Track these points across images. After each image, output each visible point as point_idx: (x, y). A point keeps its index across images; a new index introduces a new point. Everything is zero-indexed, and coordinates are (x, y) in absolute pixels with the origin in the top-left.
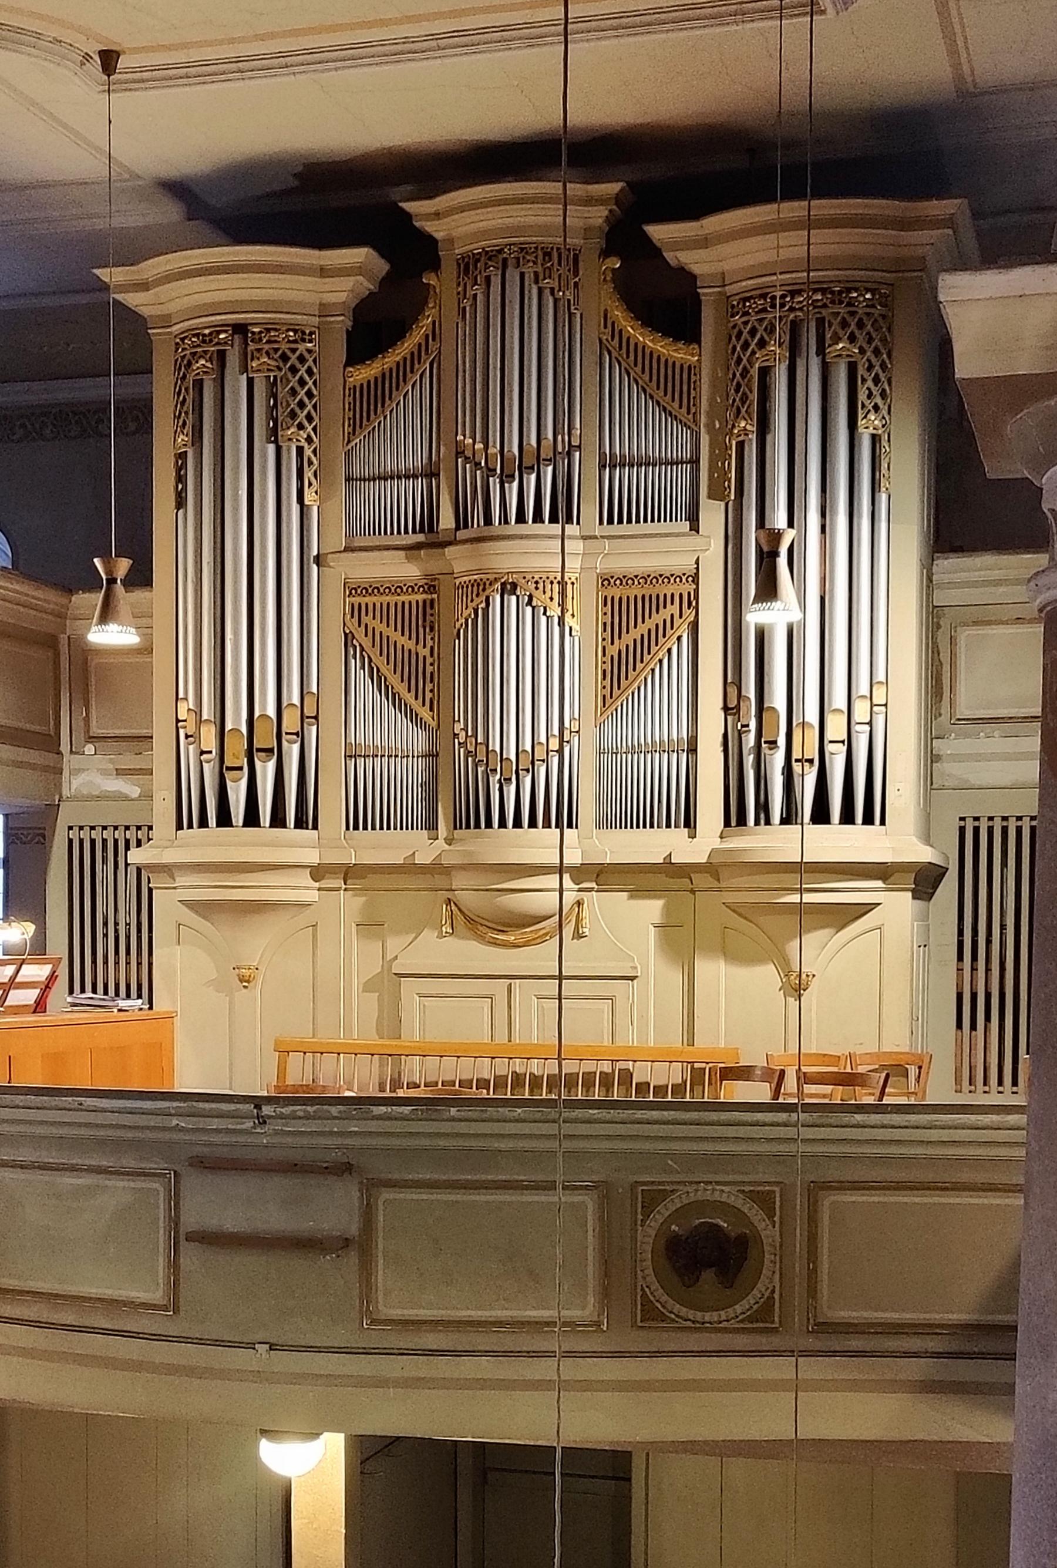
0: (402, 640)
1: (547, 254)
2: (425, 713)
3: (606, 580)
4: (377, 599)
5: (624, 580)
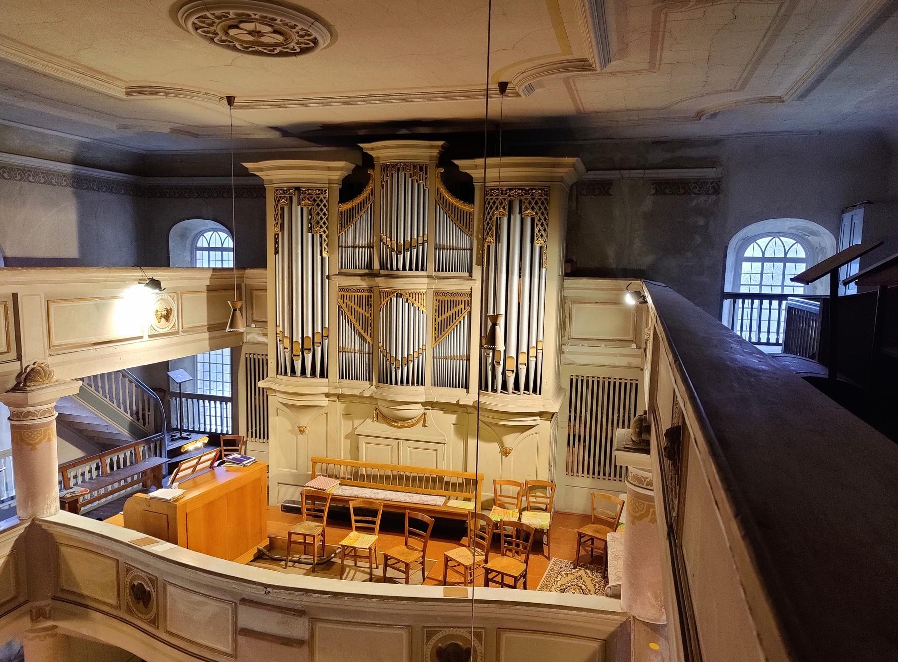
0: (360, 310)
1: (415, 167)
2: (368, 339)
3: (437, 293)
4: (350, 294)
5: (444, 294)
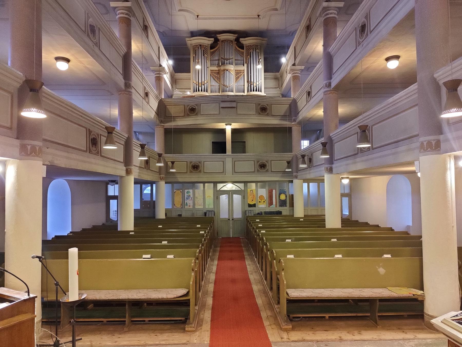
5: (237, 70)
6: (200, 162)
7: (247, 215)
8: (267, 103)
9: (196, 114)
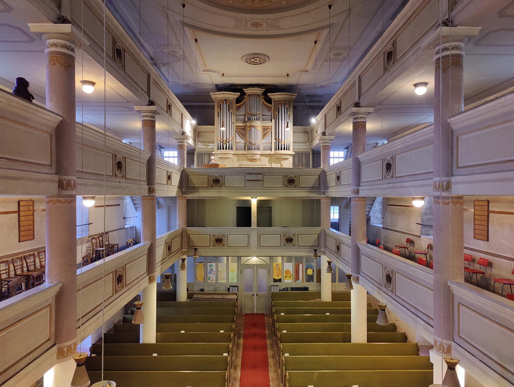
6: (223, 236)
7: (272, 291)
8: (295, 175)
9: (221, 186)
